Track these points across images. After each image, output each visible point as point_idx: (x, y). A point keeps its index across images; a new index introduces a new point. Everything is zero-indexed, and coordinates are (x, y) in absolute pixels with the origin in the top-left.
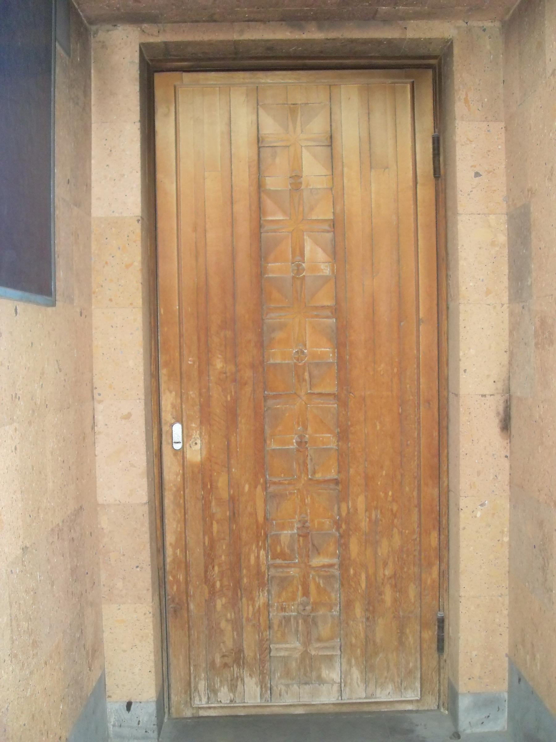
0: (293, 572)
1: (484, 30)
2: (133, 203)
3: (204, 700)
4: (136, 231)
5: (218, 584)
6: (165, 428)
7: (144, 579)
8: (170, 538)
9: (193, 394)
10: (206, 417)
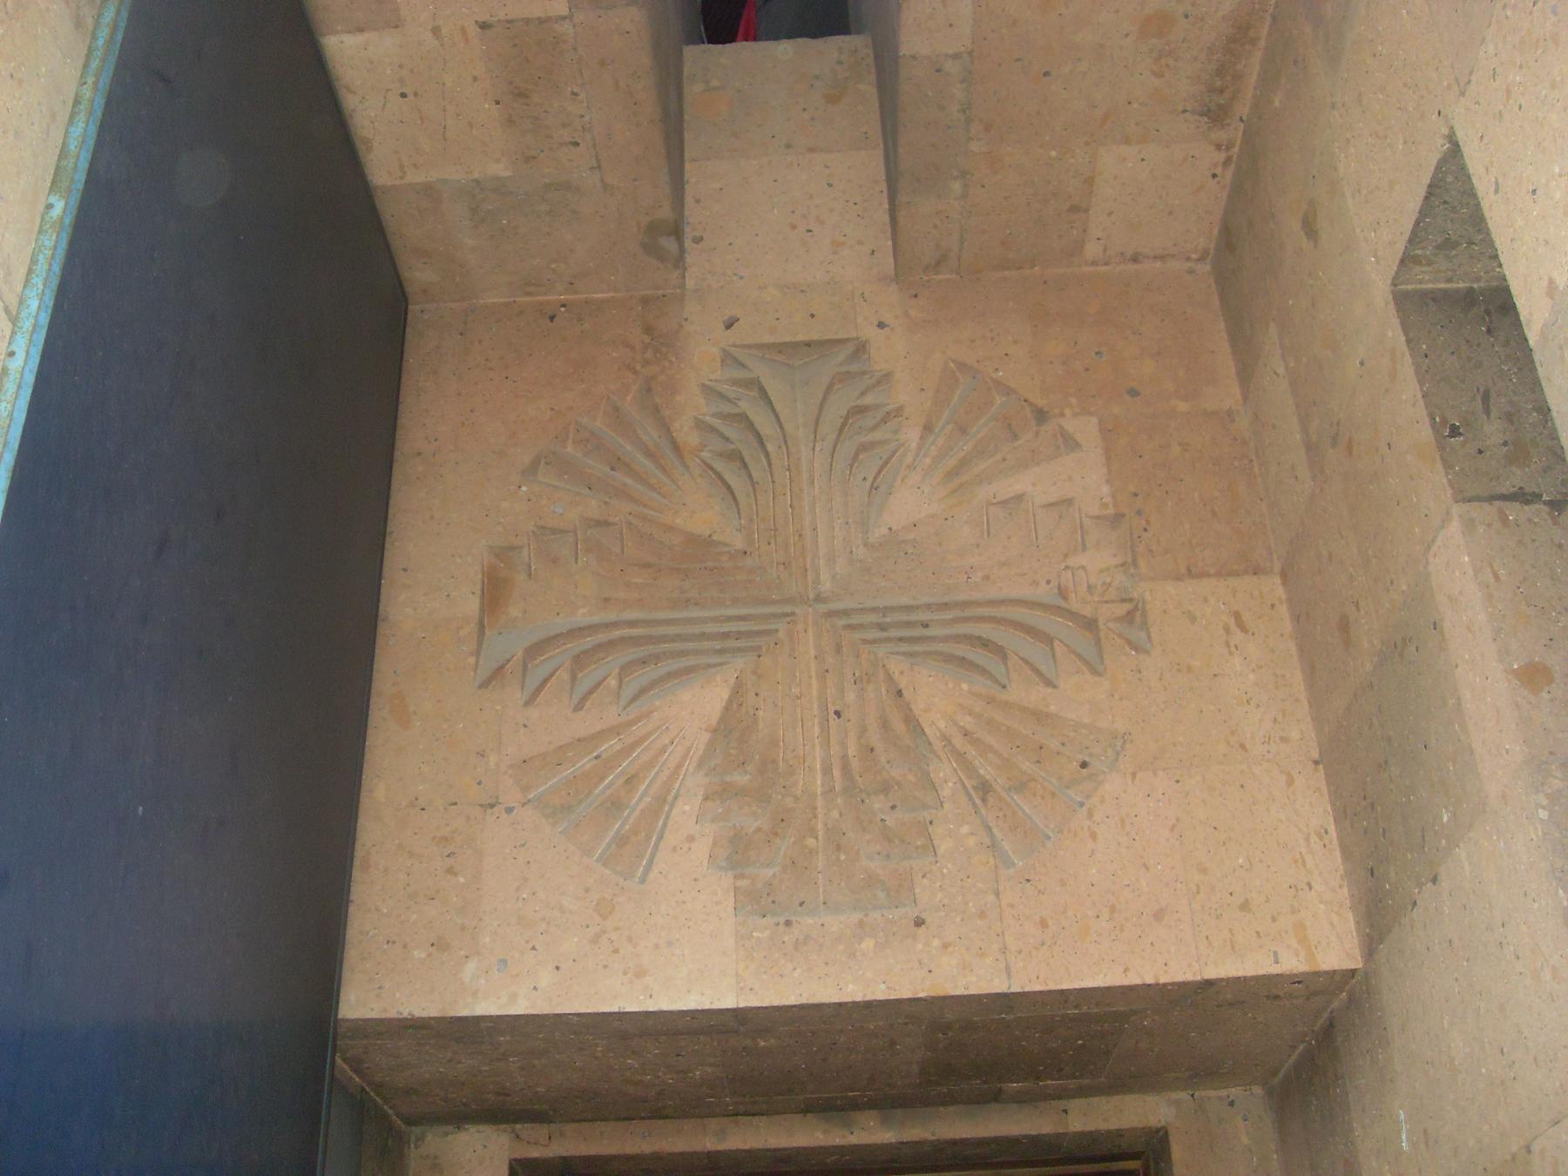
1: (1232, 1104)
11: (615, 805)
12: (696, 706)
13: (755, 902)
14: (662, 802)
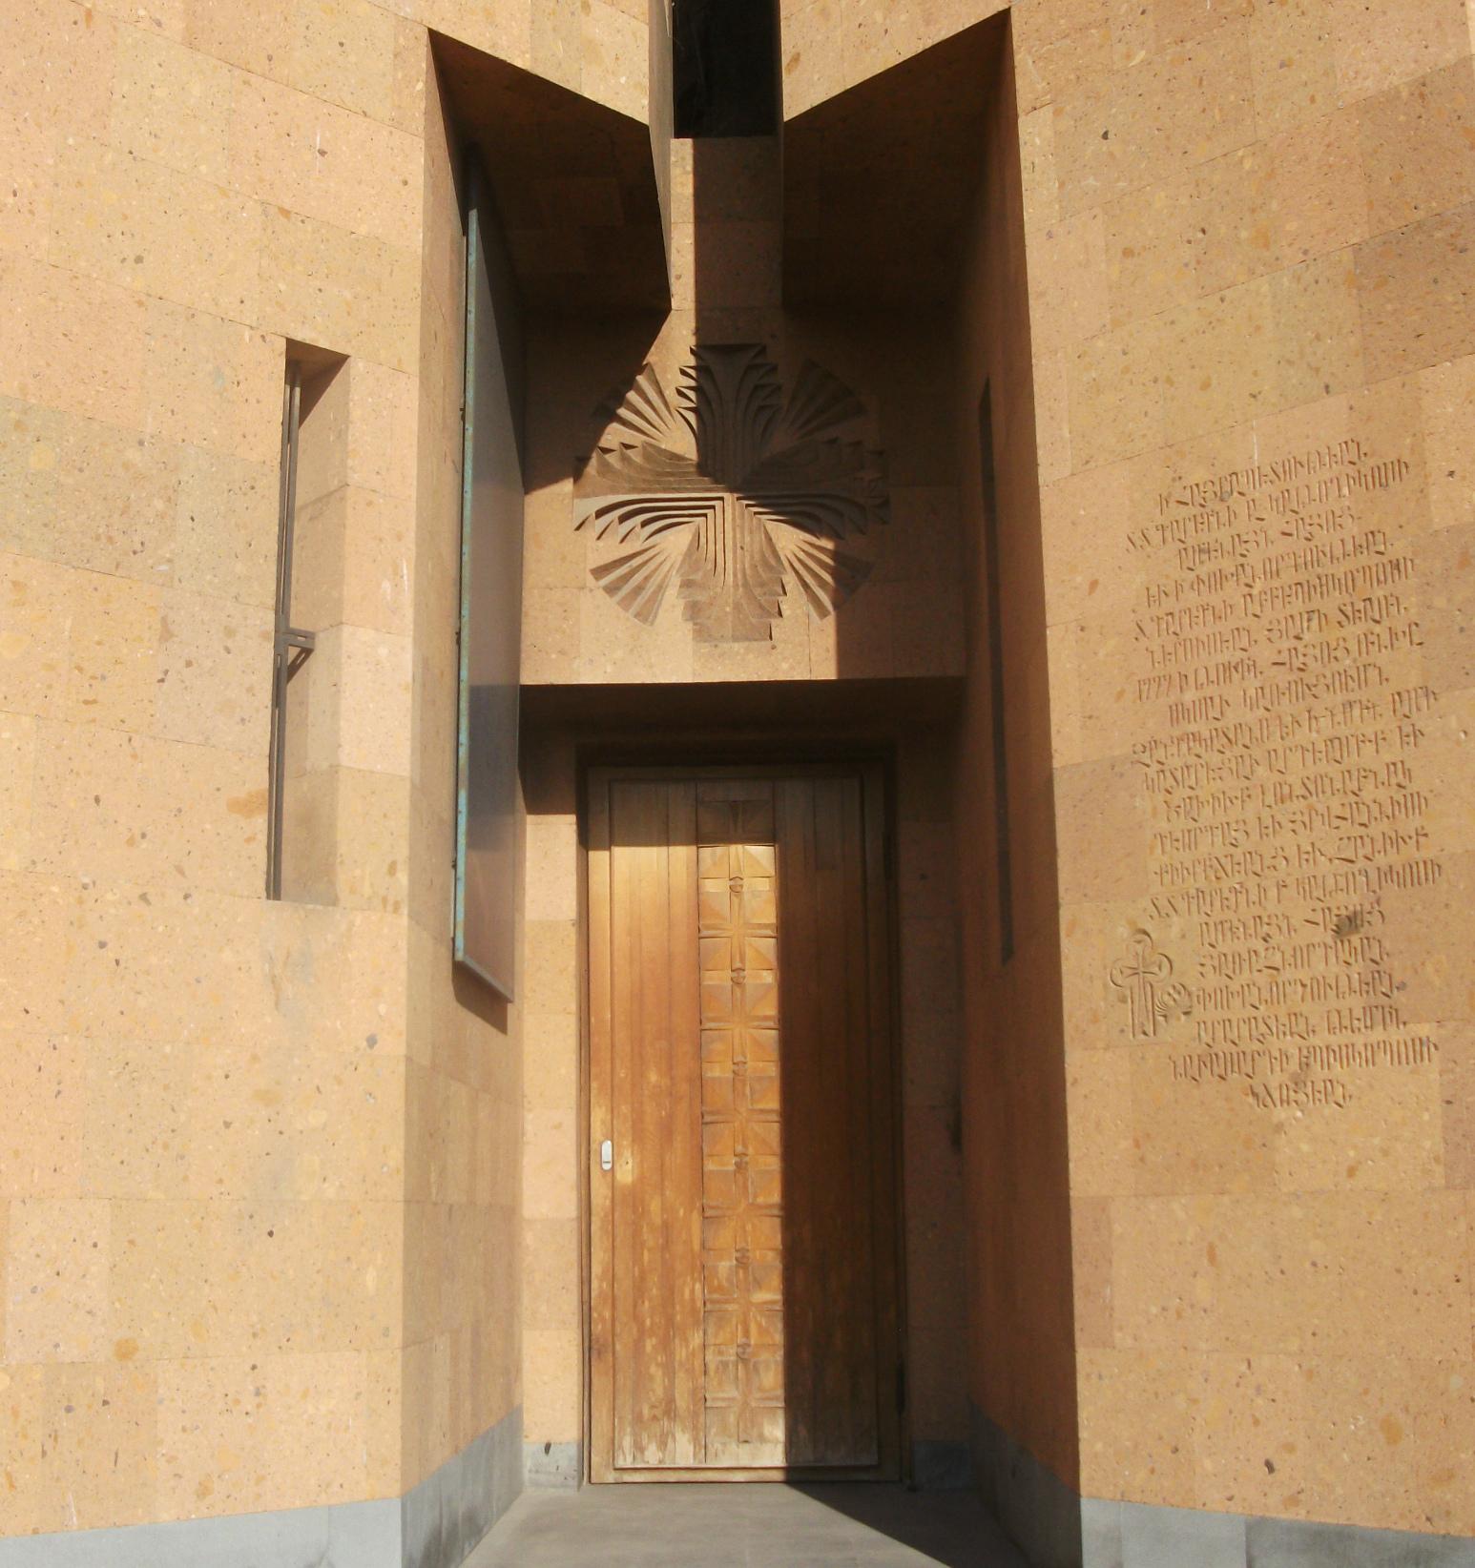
0: (730, 1307)
2: (569, 908)
3: (629, 1459)
4: (571, 936)
5: (648, 1322)
6: (593, 1146)
7: (569, 1304)
8: (596, 1269)
9: (625, 1109)
10: (638, 1136)
11: (638, 590)
12: (676, 541)
13: (702, 634)
14: (661, 588)
